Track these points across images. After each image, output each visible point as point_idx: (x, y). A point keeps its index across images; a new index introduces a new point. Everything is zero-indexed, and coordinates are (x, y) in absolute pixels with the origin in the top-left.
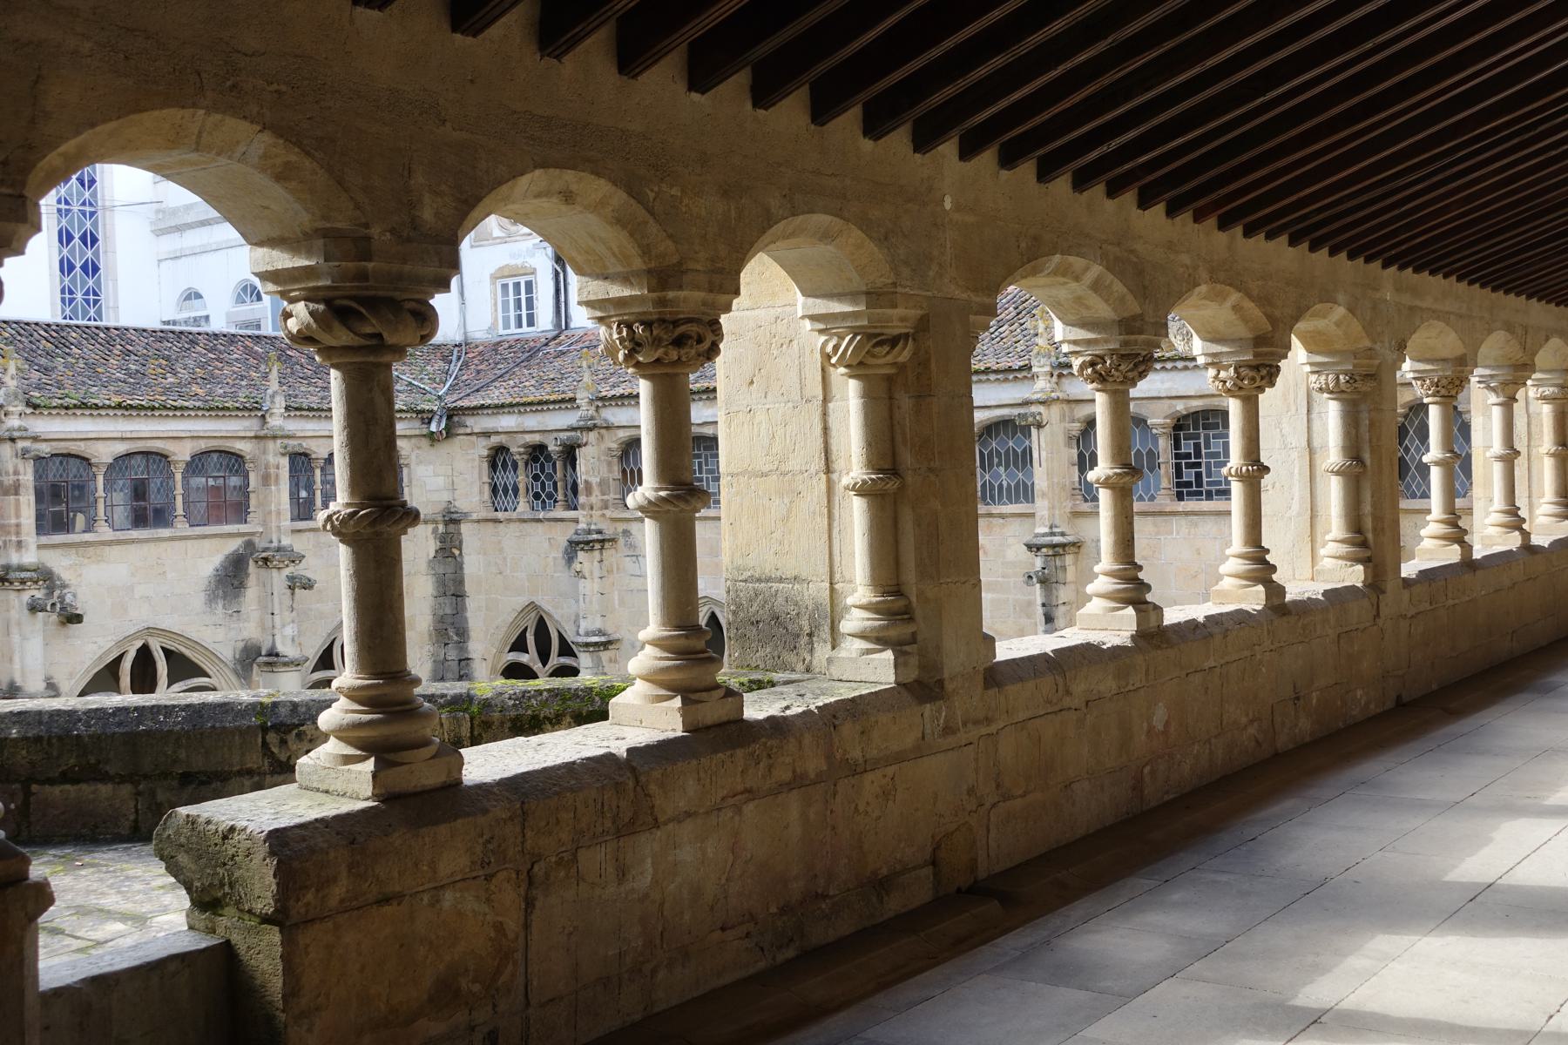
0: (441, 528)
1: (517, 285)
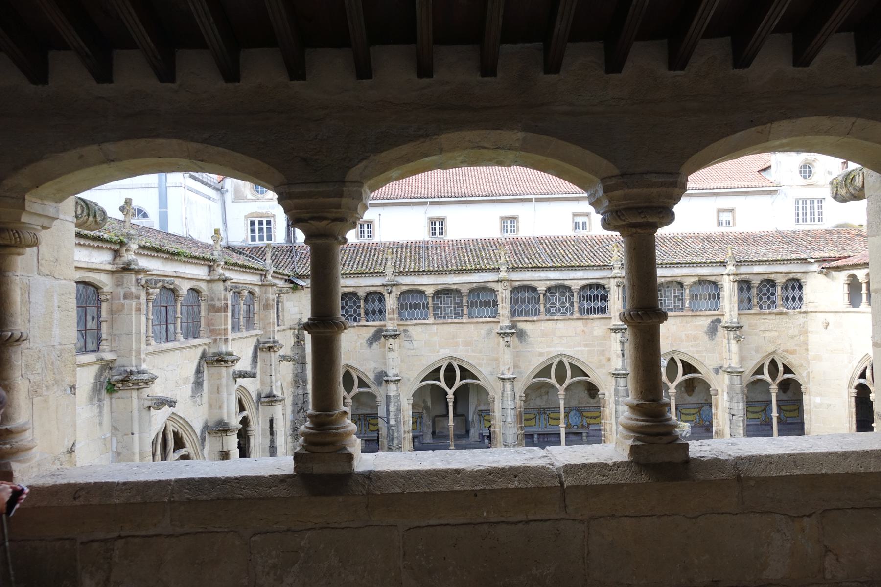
0: (296, 331)
1: (261, 223)
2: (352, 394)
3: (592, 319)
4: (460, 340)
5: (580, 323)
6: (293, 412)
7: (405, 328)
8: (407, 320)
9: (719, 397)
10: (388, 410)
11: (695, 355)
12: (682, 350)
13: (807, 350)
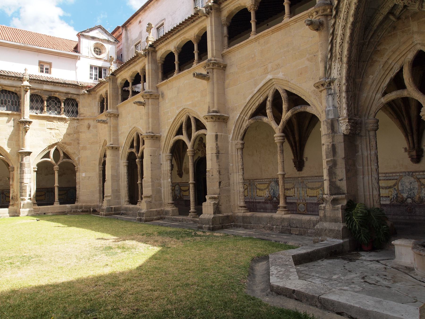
13: (79, 143)
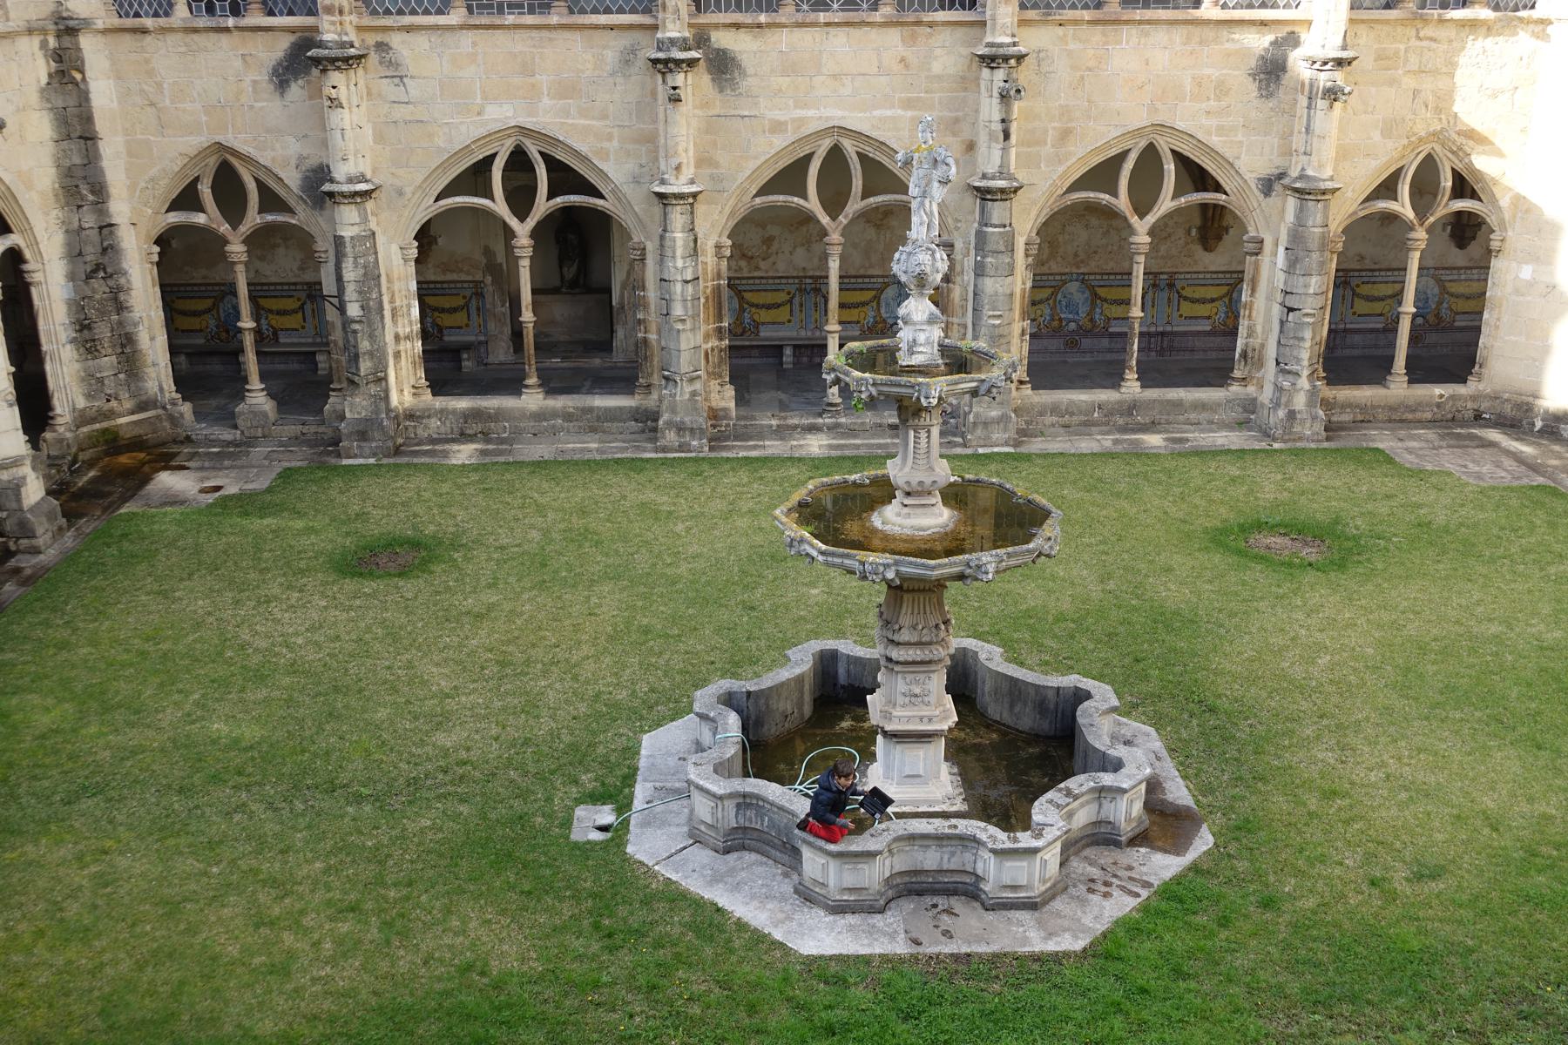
0: (52, 42)
2: (245, 228)
3: (931, 25)
4: (543, 80)
5: (893, 36)
6: (71, 277)
7: (379, 37)
8: (388, 12)
9: (1265, 259)
10: (339, 278)
11: (1215, 141)
12: (1180, 125)
